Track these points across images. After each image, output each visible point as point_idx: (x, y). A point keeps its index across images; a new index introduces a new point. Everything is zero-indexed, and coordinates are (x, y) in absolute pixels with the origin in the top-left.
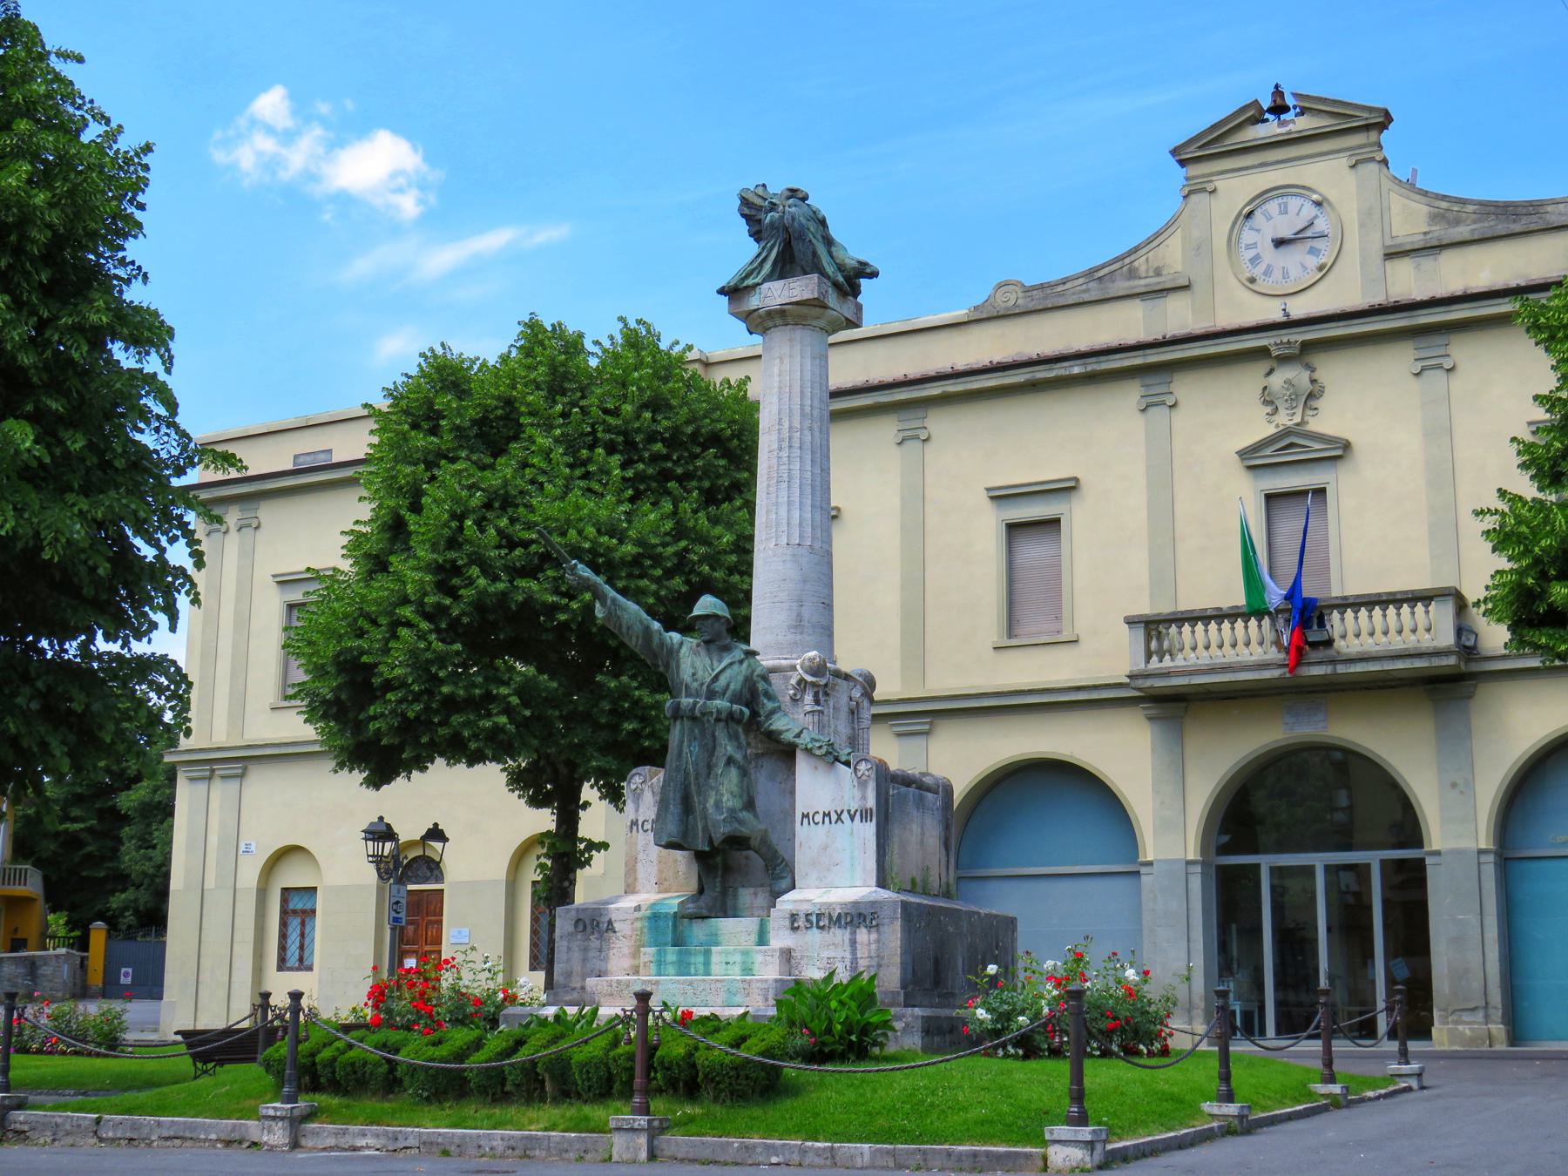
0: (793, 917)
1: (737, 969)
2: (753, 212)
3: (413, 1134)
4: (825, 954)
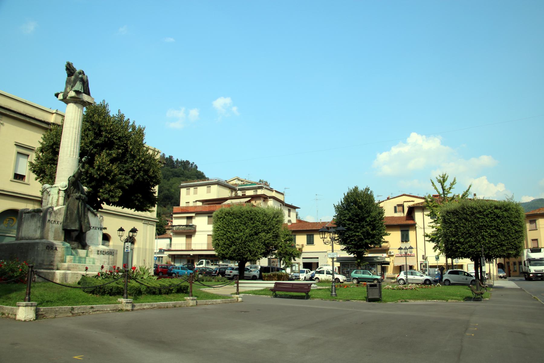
0: (98, 251)
1: (91, 263)
2: (70, 70)
3: (155, 304)
4: (104, 260)
